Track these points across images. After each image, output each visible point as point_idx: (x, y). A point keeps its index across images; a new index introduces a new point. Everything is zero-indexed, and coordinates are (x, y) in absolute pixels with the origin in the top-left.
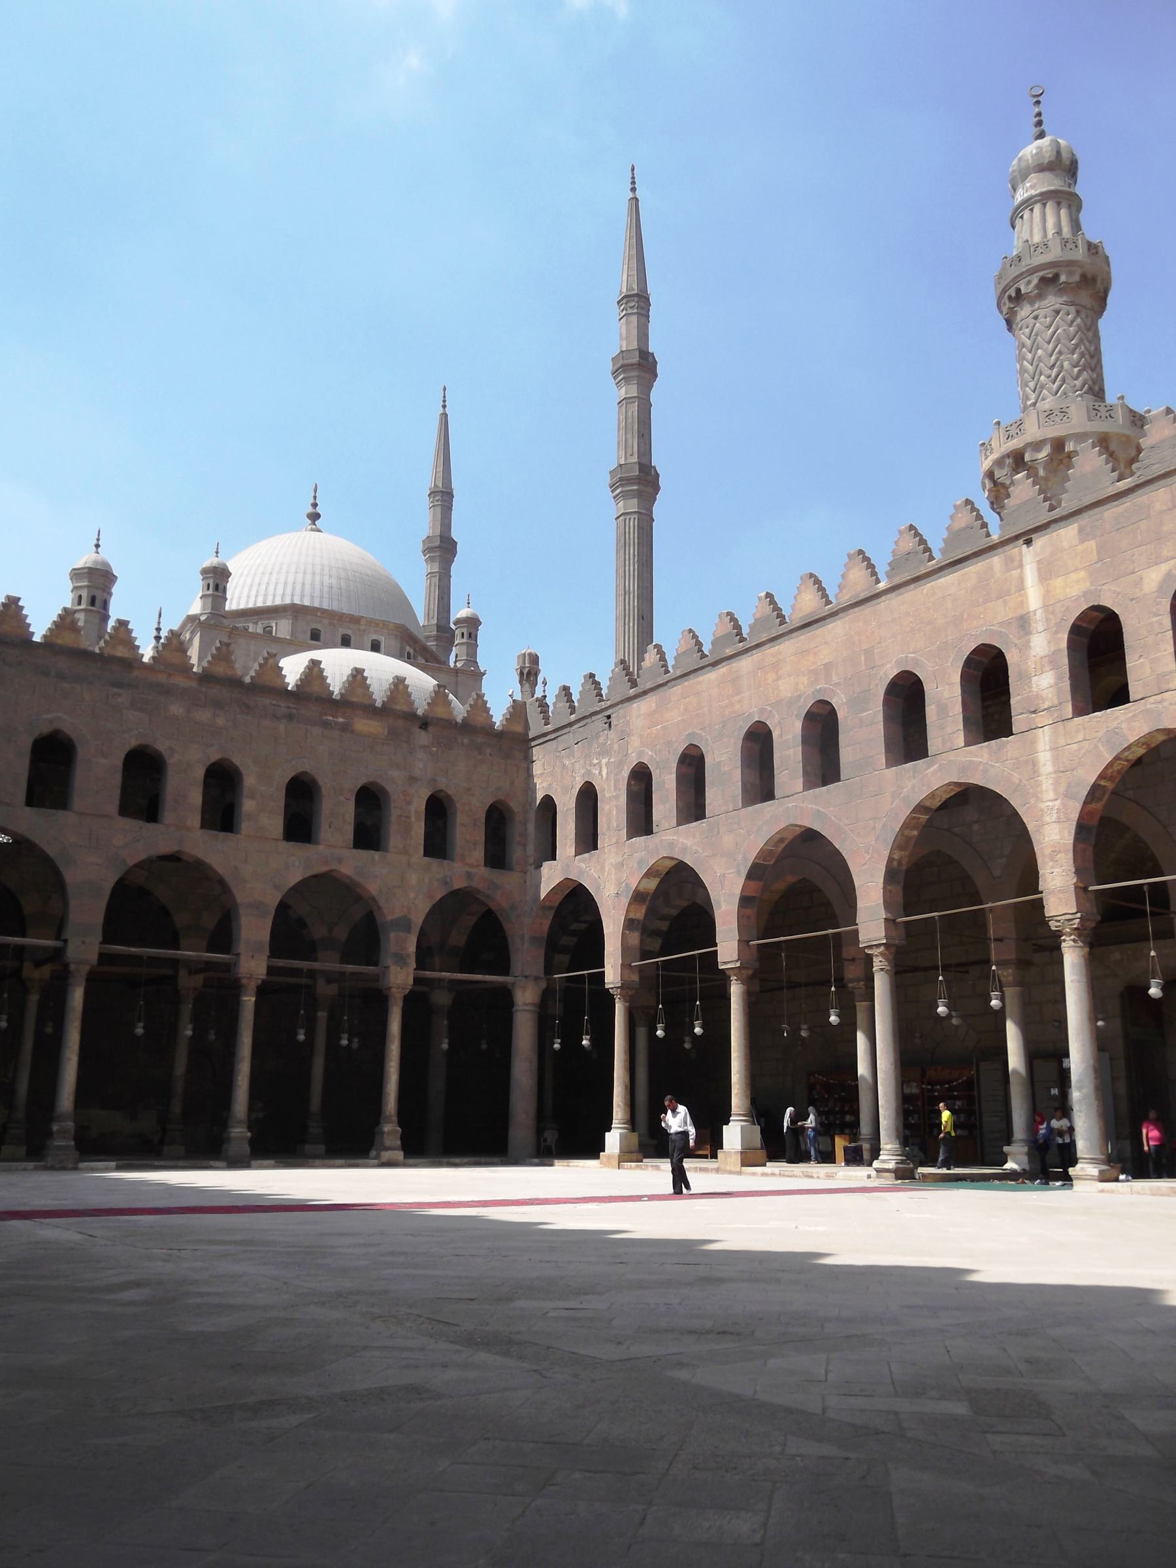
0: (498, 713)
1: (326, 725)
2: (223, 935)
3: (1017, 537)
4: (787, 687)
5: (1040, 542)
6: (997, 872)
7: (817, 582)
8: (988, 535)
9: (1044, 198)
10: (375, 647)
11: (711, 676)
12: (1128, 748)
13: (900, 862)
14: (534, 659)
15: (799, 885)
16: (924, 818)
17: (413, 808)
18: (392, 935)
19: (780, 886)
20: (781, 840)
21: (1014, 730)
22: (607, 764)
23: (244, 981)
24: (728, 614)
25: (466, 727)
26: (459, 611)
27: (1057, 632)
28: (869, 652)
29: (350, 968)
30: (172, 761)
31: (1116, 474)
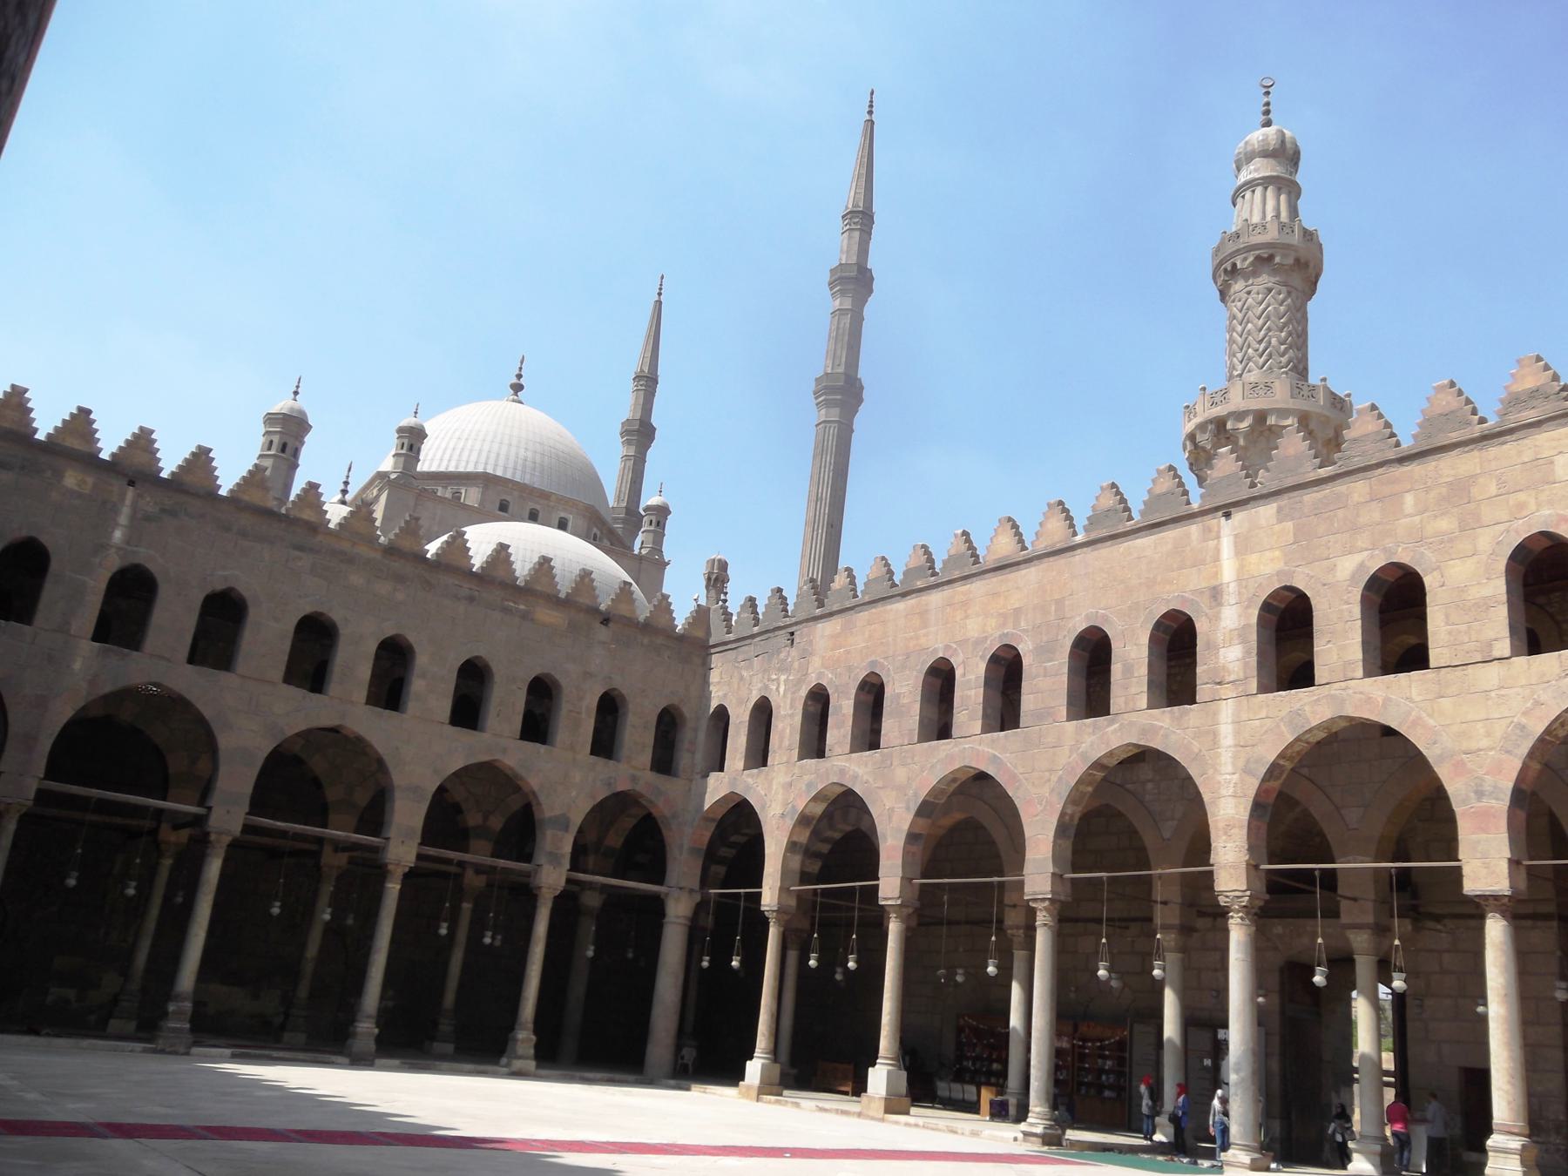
0: (681, 617)
1: (506, 610)
2: (374, 817)
3: (1217, 509)
4: (973, 628)
5: (1239, 516)
6: (1167, 835)
7: (1015, 526)
8: (1188, 503)
9: (1266, 182)
10: (562, 526)
11: (900, 606)
12: (1310, 730)
13: (1072, 817)
14: (723, 566)
15: (969, 826)
16: (1100, 775)
18: (549, 833)
19: (947, 822)
20: (954, 780)
21: (1198, 699)
23: (390, 867)
24: (923, 546)
25: (647, 627)
26: (649, 499)
27: (1248, 607)
28: (1060, 603)
29: (502, 863)
30: (344, 632)
31: (1318, 461)
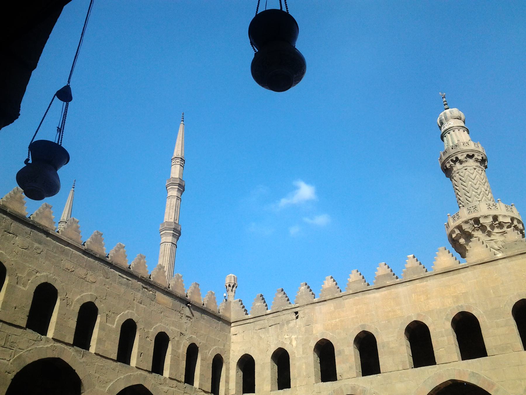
4: (434, 304)
17: (180, 351)
20: (439, 388)
22: (295, 338)
